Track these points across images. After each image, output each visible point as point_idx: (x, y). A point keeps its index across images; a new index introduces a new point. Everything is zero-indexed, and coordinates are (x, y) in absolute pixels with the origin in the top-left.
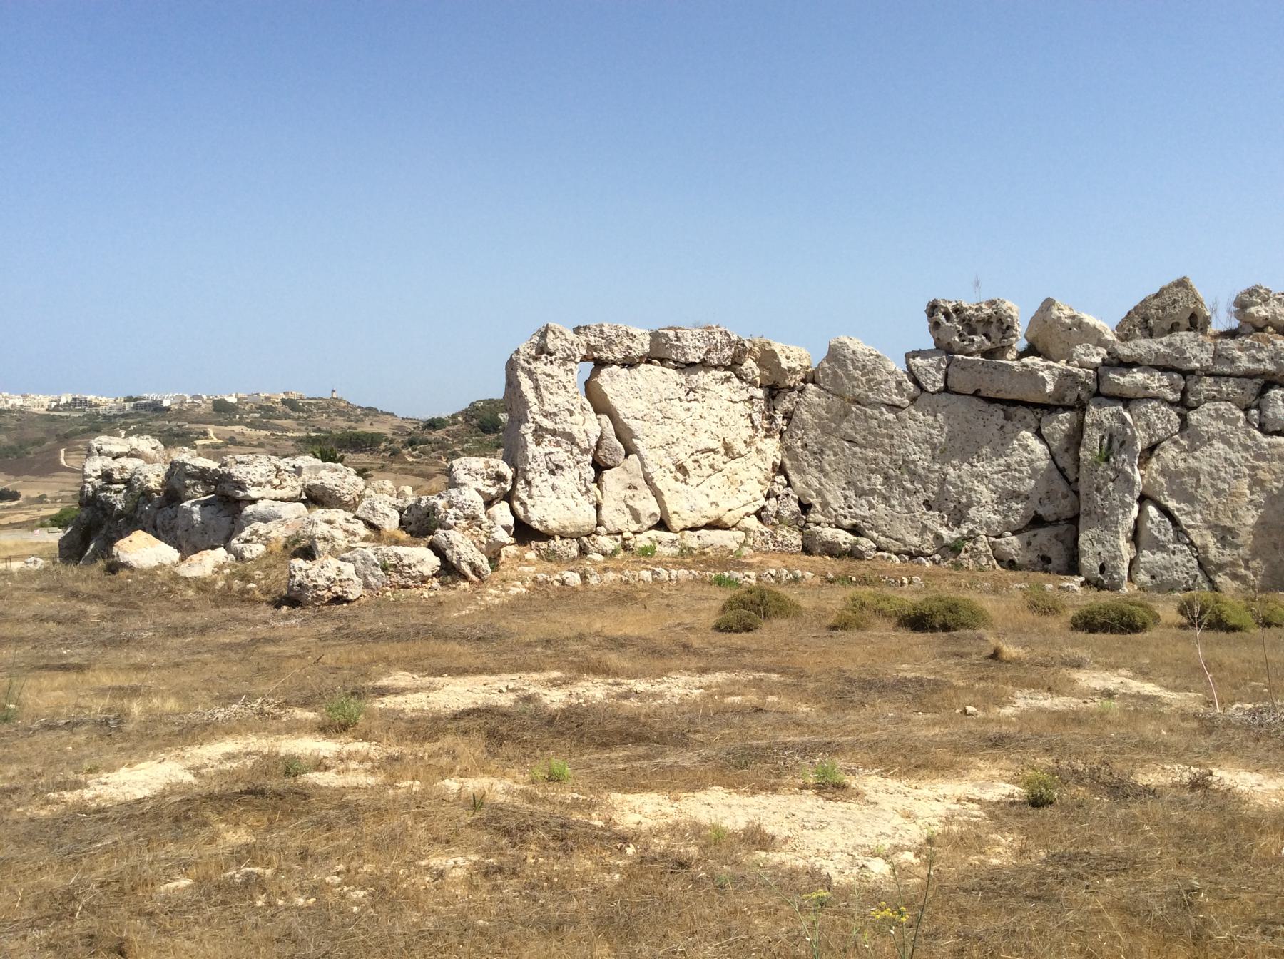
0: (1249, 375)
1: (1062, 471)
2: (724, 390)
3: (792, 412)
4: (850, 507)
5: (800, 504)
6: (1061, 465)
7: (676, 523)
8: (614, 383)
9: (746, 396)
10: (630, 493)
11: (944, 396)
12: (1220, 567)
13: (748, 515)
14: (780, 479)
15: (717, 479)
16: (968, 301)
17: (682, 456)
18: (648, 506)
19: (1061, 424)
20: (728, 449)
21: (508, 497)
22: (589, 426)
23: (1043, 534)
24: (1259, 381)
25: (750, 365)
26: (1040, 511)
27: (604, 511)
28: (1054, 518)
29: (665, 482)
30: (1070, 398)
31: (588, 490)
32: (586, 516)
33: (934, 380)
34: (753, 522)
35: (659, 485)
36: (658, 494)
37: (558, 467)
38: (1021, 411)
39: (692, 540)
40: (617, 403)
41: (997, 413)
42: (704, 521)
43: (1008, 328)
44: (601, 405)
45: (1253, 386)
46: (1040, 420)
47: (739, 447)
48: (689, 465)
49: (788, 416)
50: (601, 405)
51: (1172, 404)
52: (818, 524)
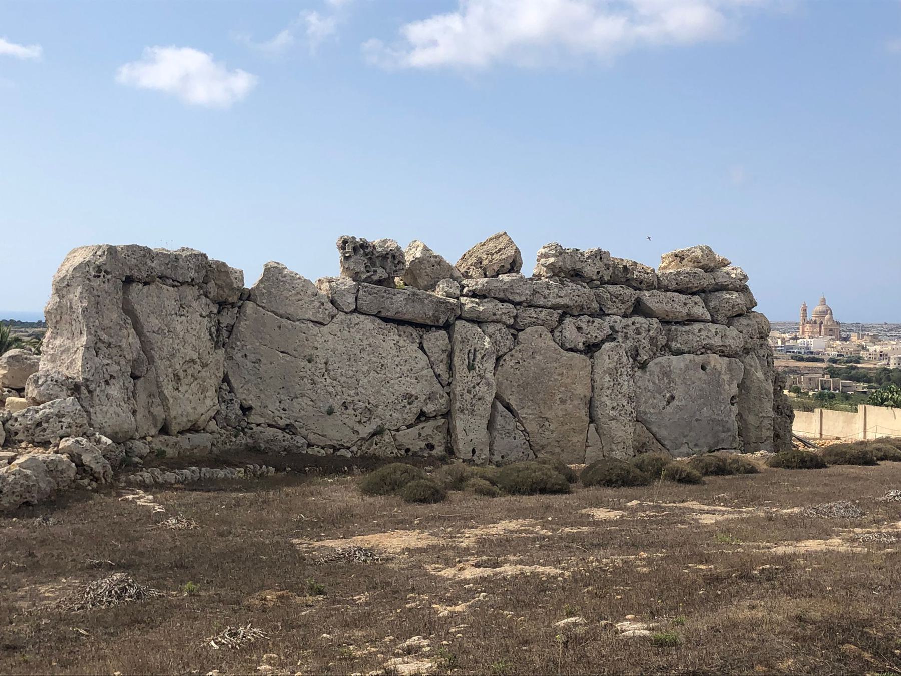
0: (555, 307)
1: (438, 376)
3: (233, 326)
4: (284, 410)
5: (242, 407)
6: (438, 371)
7: (175, 428)
11: (356, 315)
12: (543, 447)
14: (225, 386)
16: (374, 238)
19: (437, 340)
23: (428, 427)
24: (560, 312)
26: (425, 409)
28: (435, 413)
30: (442, 321)
31: (129, 398)
33: (349, 301)
34: (213, 425)
37: (111, 376)
38: (410, 329)
43: (399, 262)
45: (556, 315)
46: (421, 337)
48: (182, 374)
51: (509, 327)
52: (258, 425)
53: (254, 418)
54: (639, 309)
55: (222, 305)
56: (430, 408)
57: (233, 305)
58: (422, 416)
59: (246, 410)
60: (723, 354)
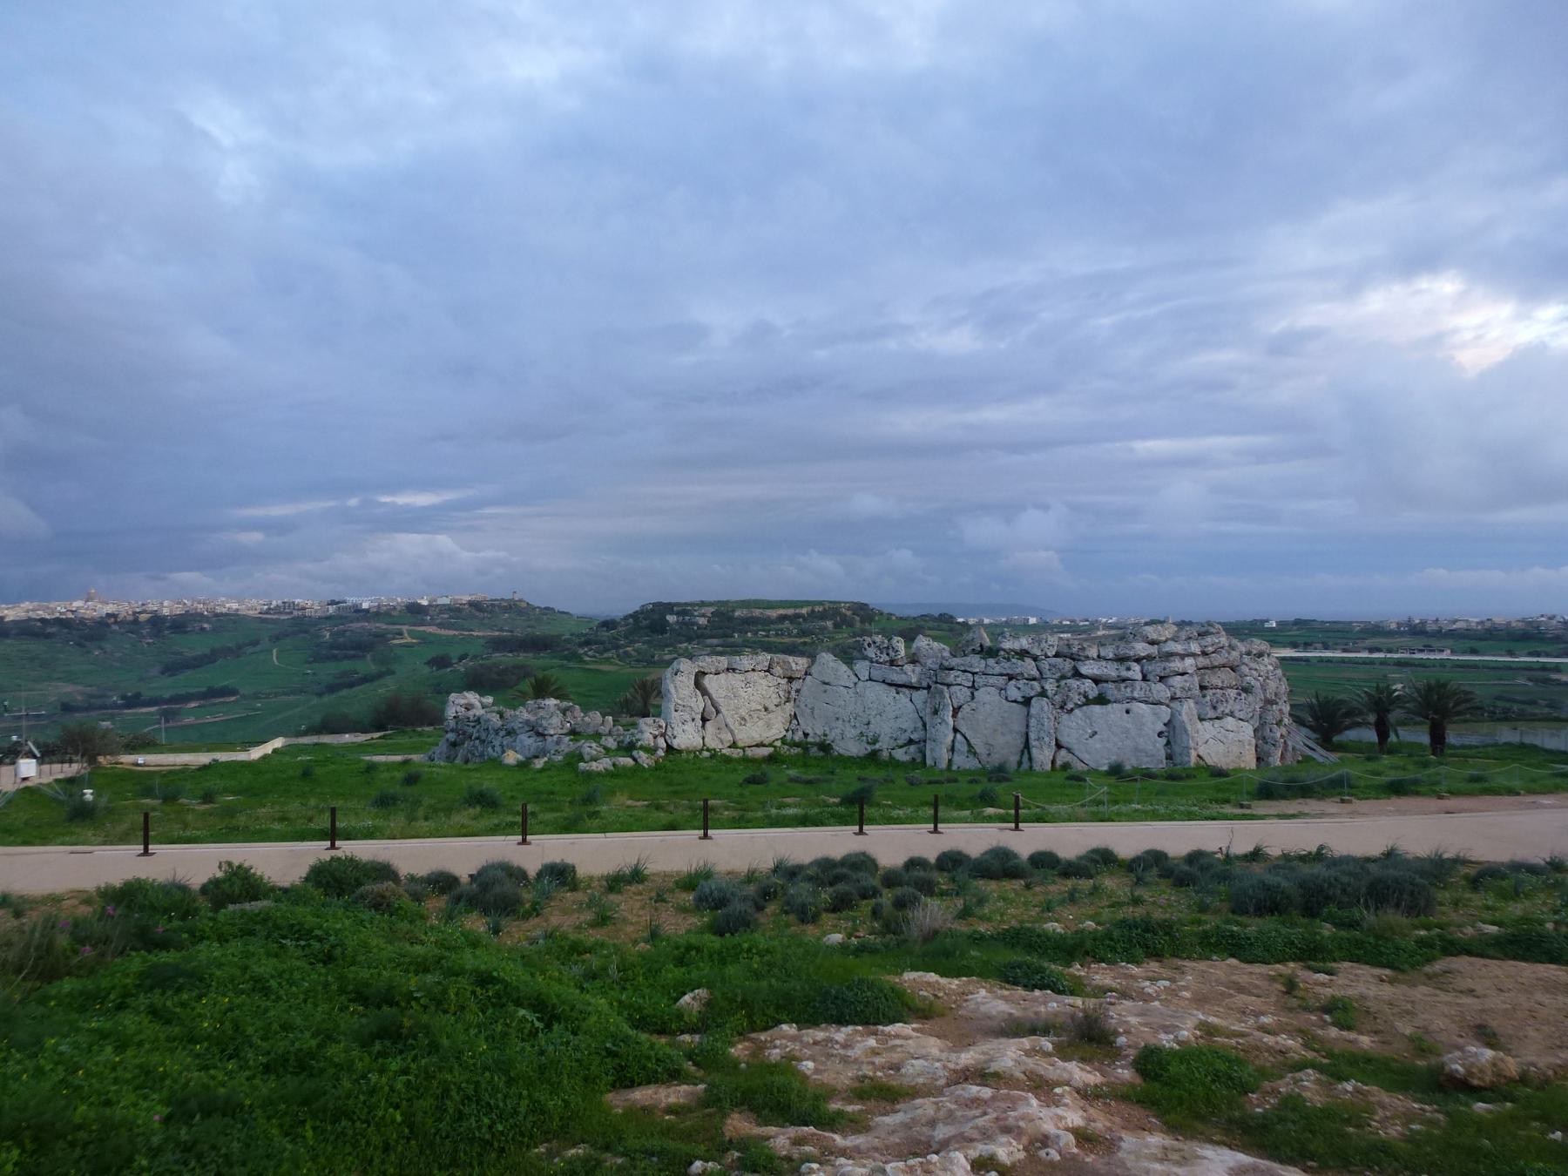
2: (764, 682)
7: (740, 744)
8: (708, 681)
15: (761, 723)
18: (728, 738)
19: (920, 696)
21: (663, 735)
22: (699, 703)
23: (913, 748)
25: (778, 670)
29: (734, 726)
30: (924, 684)
32: (698, 742)
34: (778, 744)
36: (732, 732)
39: (749, 752)
40: (712, 691)
41: (893, 689)
44: (705, 692)
49: (798, 691)
50: (705, 692)
53: (810, 739)
54: (1077, 674)
55: (791, 679)
56: (915, 736)
58: (911, 742)
59: (806, 735)
60: (1146, 702)
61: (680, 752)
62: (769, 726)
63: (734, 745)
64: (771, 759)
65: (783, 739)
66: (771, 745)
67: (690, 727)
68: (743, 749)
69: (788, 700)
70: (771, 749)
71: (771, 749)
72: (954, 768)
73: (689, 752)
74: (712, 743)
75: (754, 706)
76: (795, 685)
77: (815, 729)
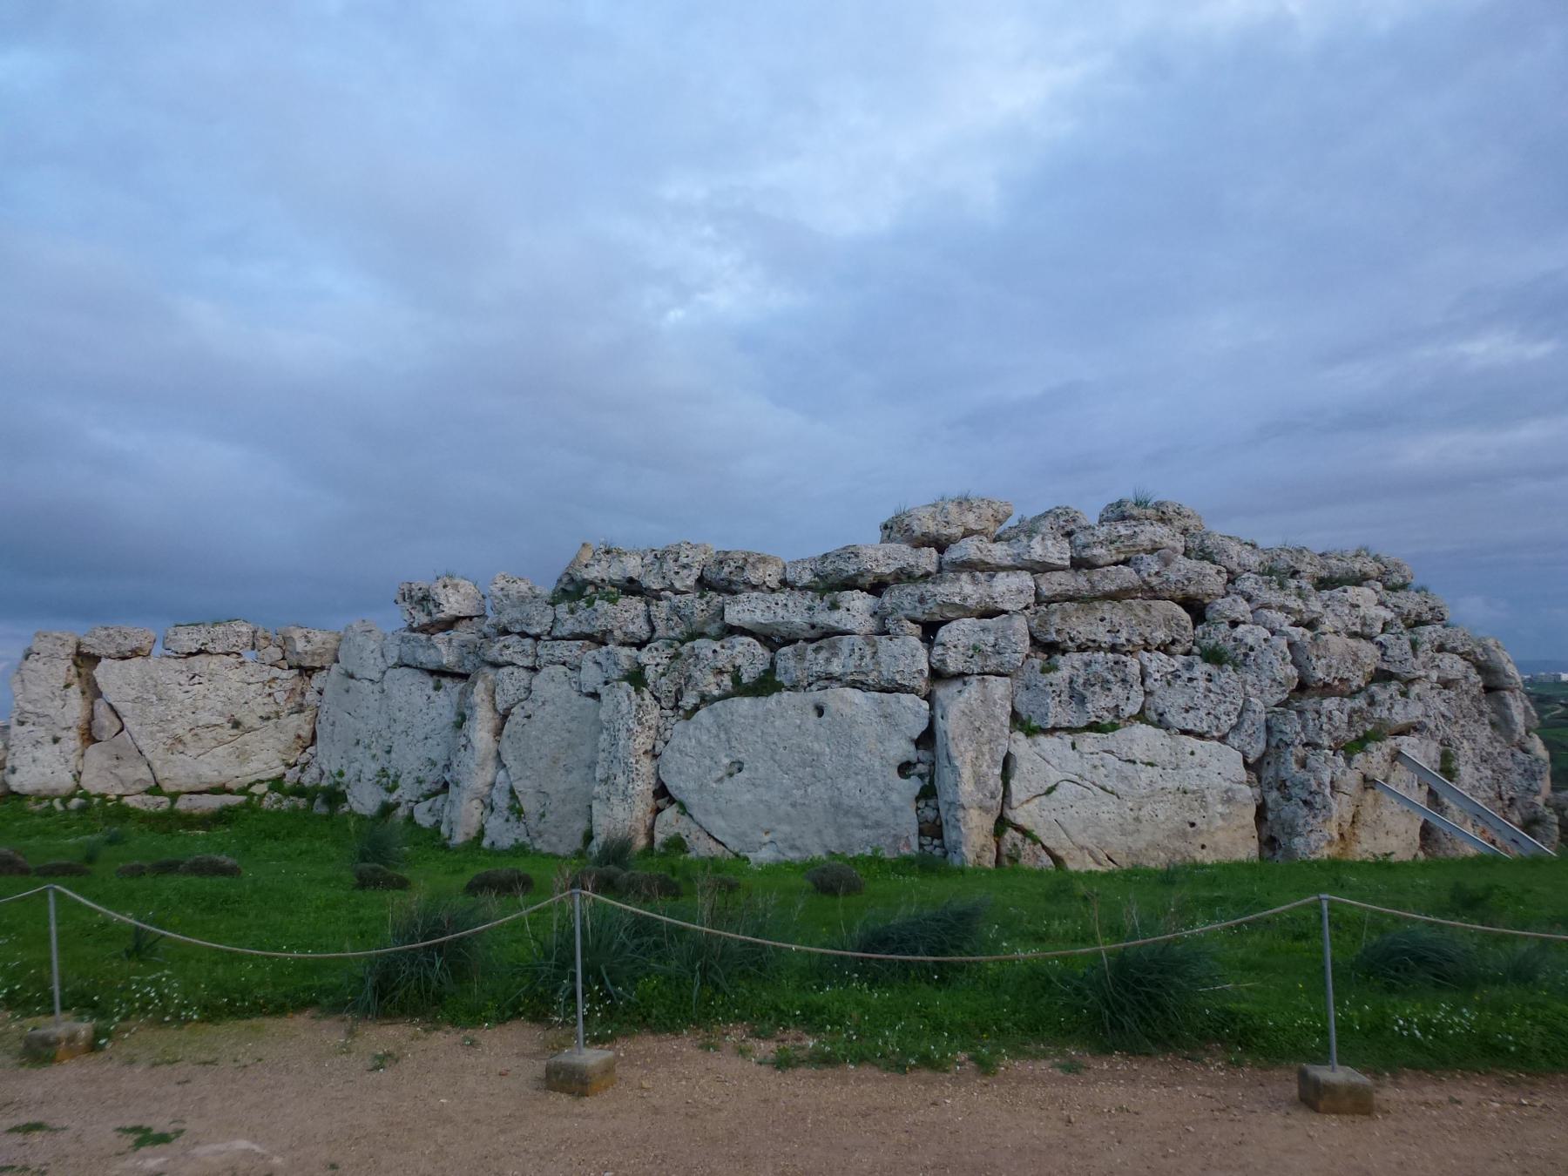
7: (168, 787)
9: (267, 678)
10: (115, 762)
13: (261, 782)
17: (180, 732)
20: (236, 724)
27: (84, 778)
32: (65, 781)
35: (149, 756)
38: (446, 682)
39: (183, 804)
41: (431, 682)
42: (203, 787)
47: (250, 720)
48: (188, 738)
57: (322, 668)
61: (19, 797)
62: (242, 756)
63: (155, 790)
64: (222, 817)
65: (276, 784)
66: (243, 791)
67: (48, 753)
68: (174, 797)
69: (300, 709)
70: (242, 798)
71: (242, 798)
72: (486, 843)
73: (40, 798)
74: (94, 783)
75: (205, 717)
76: (317, 681)
77: (327, 761)
